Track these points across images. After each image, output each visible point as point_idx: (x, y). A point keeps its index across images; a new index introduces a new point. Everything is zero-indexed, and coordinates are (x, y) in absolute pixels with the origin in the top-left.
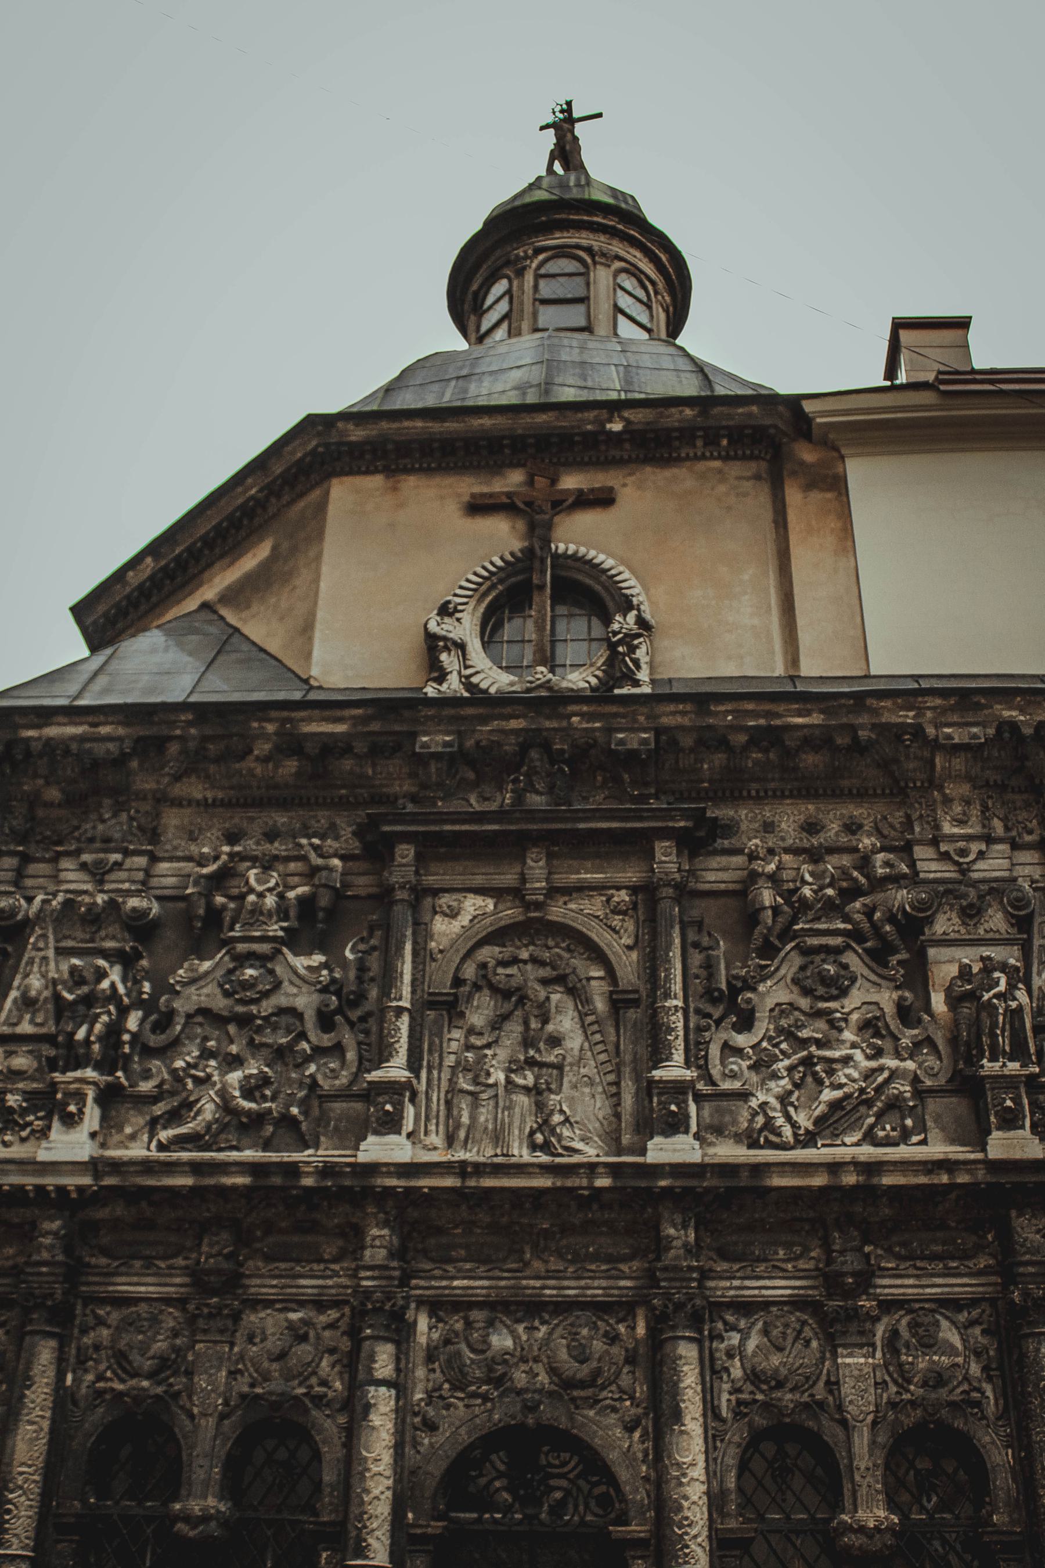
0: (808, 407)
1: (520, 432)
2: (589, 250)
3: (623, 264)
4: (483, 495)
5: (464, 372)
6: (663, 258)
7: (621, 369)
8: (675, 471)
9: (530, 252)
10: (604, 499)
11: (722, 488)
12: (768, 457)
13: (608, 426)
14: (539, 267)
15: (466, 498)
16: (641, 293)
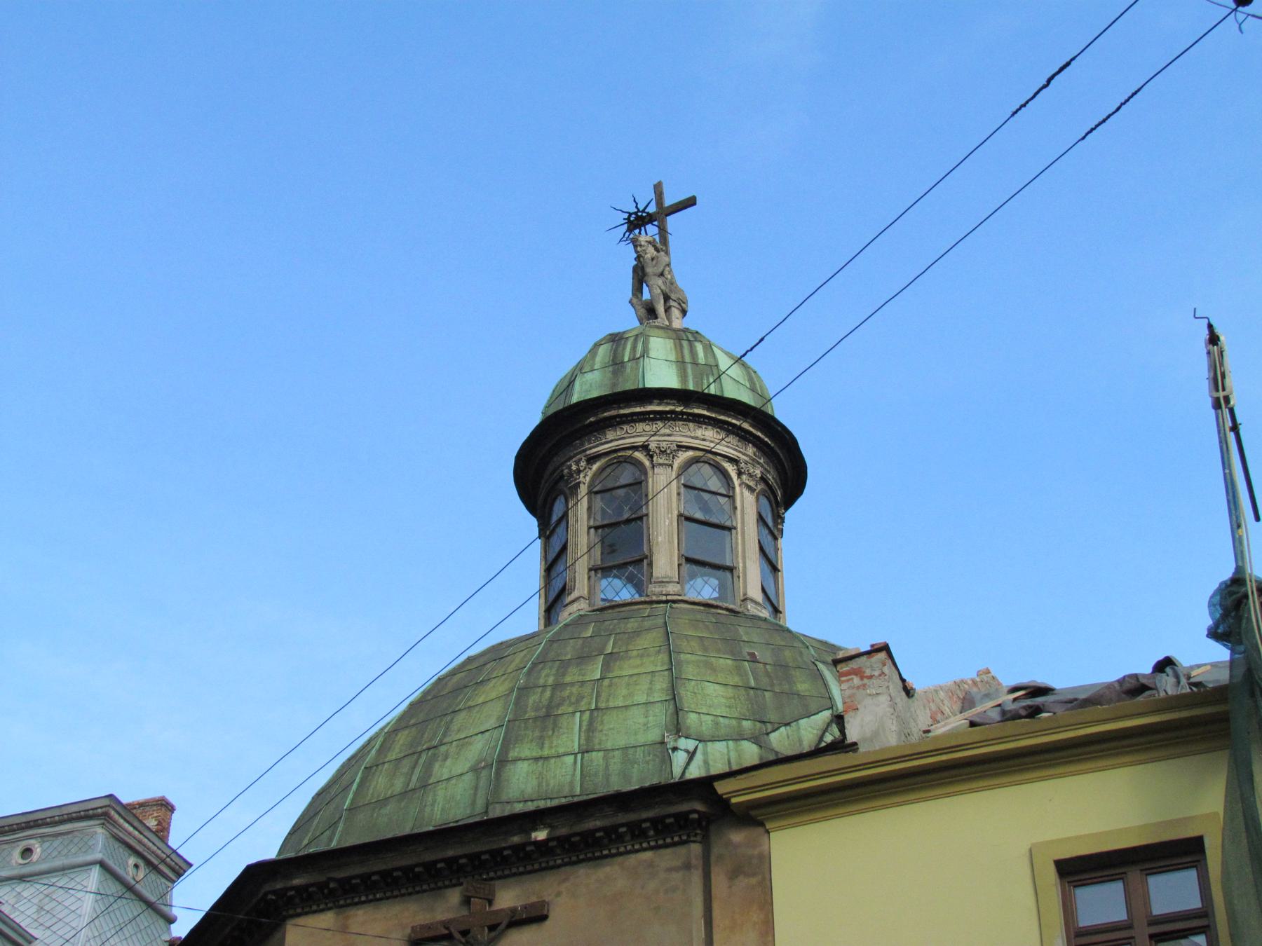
0: (722, 788)
1: (450, 853)
2: (645, 447)
3: (690, 453)
4: (422, 927)
5: (435, 743)
6: (746, 426)
7: (587, 714)
8: (608, 869)
9: (583, 464)
10: (535, 916)
11: (652, 885)
12: (699, 838)
13: (534, 835)
14: (591, 485)
15: (409, 931)
16: (715, 483)
